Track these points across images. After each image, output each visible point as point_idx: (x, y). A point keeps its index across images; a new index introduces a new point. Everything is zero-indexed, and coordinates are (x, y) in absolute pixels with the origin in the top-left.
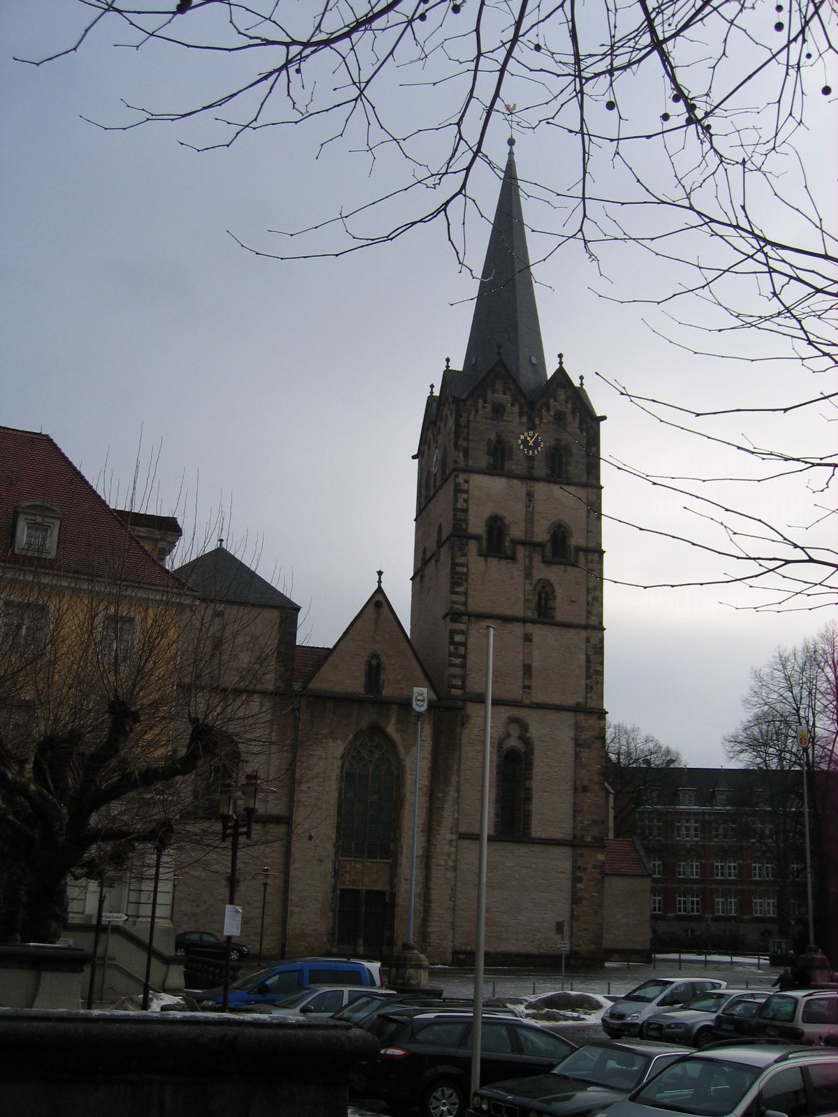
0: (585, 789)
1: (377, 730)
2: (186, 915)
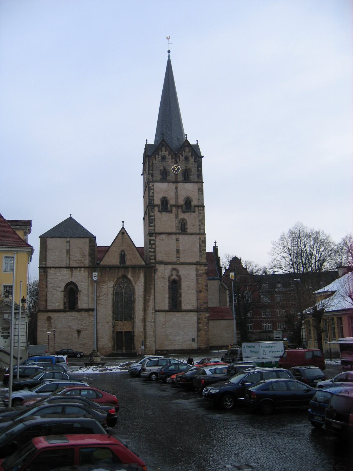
0: (201, 291)
1: (125, 277)
2: (64, 344)
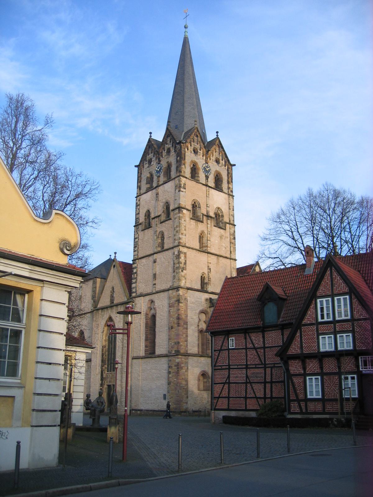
0: (172, 328)
